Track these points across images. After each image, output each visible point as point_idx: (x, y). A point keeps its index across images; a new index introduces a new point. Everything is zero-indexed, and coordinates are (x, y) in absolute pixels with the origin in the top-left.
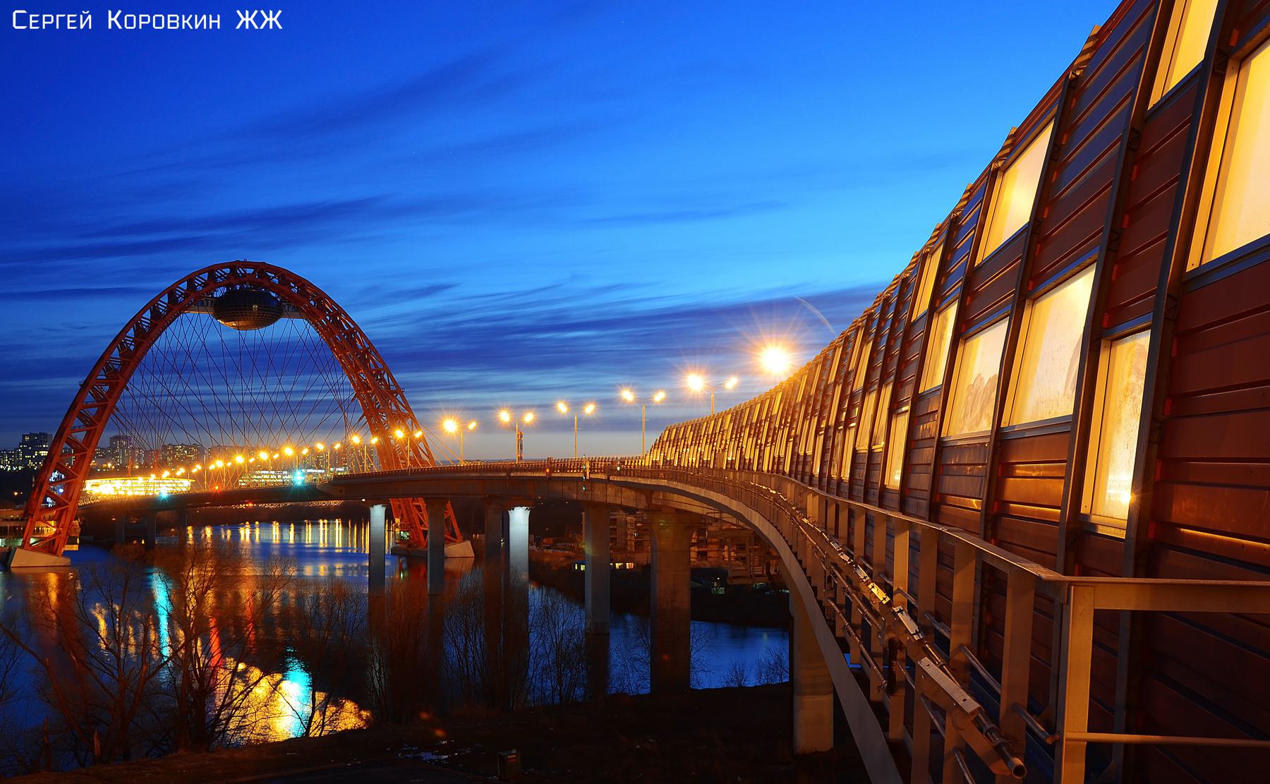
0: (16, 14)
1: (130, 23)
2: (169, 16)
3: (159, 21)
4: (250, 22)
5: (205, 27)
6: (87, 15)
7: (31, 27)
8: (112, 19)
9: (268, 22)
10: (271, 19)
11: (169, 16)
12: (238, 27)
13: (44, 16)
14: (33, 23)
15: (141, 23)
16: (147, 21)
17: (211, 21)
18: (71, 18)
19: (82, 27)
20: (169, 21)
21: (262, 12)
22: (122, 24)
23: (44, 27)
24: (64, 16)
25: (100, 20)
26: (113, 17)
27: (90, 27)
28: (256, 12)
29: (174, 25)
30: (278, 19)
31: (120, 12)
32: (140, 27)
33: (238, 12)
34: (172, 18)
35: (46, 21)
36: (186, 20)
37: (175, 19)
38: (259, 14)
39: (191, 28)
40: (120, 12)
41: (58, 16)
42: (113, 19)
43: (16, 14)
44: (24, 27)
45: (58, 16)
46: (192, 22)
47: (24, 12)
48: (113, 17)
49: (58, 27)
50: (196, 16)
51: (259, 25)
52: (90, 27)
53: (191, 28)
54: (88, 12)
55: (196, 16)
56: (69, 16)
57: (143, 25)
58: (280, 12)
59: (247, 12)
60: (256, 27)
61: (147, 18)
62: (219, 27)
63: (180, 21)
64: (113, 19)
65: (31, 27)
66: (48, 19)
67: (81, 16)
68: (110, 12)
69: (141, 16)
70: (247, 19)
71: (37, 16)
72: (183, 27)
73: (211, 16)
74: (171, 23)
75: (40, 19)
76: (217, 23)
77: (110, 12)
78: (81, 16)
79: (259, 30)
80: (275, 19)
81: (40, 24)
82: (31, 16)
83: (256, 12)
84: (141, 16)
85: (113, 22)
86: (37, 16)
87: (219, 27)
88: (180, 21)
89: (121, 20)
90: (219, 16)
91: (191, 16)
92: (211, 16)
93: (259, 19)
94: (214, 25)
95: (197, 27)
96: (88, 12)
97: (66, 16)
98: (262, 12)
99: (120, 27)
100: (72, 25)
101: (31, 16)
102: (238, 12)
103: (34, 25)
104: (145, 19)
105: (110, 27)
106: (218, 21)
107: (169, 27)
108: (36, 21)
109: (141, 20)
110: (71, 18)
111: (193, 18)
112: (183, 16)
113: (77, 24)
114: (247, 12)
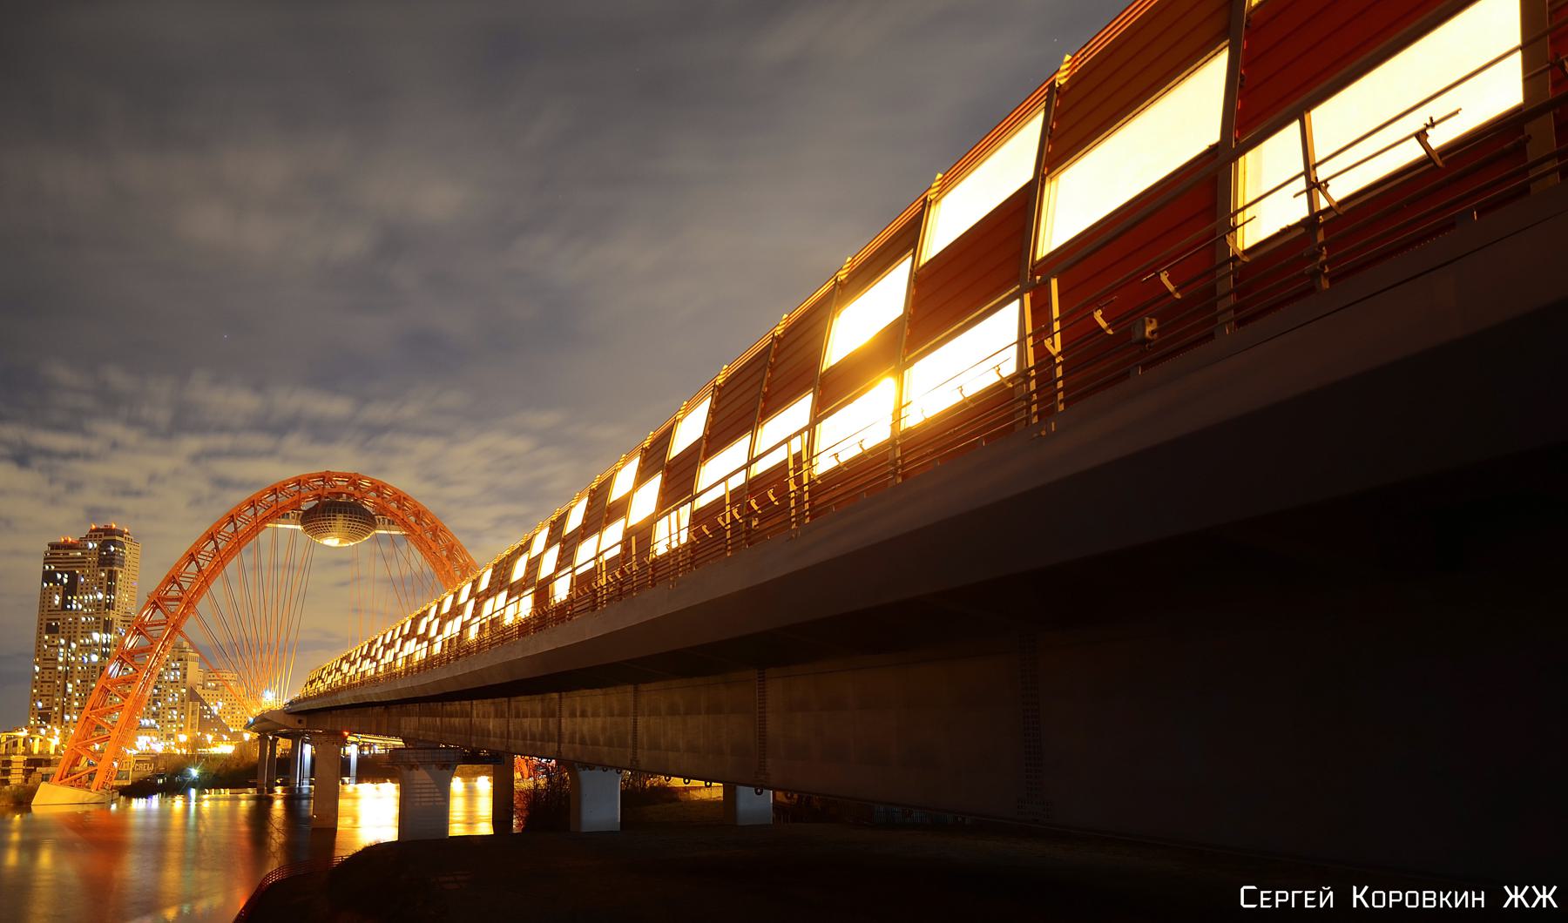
1: (1379, 901)
2: (1424, 893)
3: (1412, 899)
5: (1467, 906)
6: (1328, 891)
7: (1262, 906)
8: (1357, 896)
10: (1545, 896)
11: (1424, 893)
12: (1505, 906)
13: (1277, 893)
15: (1391, 900)
16: (1398, 898)
17: (1474, 899)
18: (1309, 896)
19: (1322, 905)
20: (1425, 899)
21: (1534, 888)
22: (1369, 902)
23: (1277, 906)
24: (1300, 892)
25: (1343, 897)
26: (1358, 893)
27: (1332, 906)
28: (1527, 888)
29: (1431, 903)
31: (1366, 888)
32: (1391, 906)
33: (1506, 888)
34: (1427, 896)
35: (1280, 898)
36: (1444, 897)
37: (1431, 896)
39: (1450, 906)
40: (1366, 888)
41: (1293, 893)
42: (1358, 896)
45: (1293, 893)
46: (1452, 899)
47: (1254, 888)
48: (1358, 893)
49: (1293, 906)
50: (1456, 893)
51: (1530, 904)
52: (1332, 906)
53: (1450, 906)
54: (1329, 888)
55: (1456, 893)
56: (1306, 893)
57: (1280, 903)
60: (1527, 906)
61: (1398, 894)
62: (1483, 906)
63: (1438, 899)
64: (1358, 896)
65: (1262, 906)
66: (1282, 896)
67: (1321, 893)
68: (1355, 888)
69: (1391, 893)
70: (1516, 896)
72: (1441, 906)
73: (1473, 893)
74: (1427, 901)
75: (1273, 896)
76: (1480, 901)
77: (1355, 888)
78: (1321, 893)
79: (1530, 909)
80: (1549, 896)
81: (1272, 902)
82: (1262, 893)
83: (1527, 888)
84: (1391, 893)
85: (1358, 900)
87: (1483, 906)
88: (1438, 899)
89: (1367, 897)
90: (1483, 893)
91: (1450, 893)
92: (1473, 893)
93: (1530, 897)
94: (1478, 903)
95: (1457, 905)
96: (1329, 888)
97: (1303, 893)
98: (1534, 888)
99: (1367, 906)
100: (1310, 903)
101: (1262, 893)
102: (1506, 888)
103: (1265, 903)
104: (1396, 896)
105: (1355, 906)
106: (1482, 899)
107: (1424, 906)
108: (1313, 899)
109: (1391, 898)
110: (1309, 896)
111: (1453, 895)
112: (1441, 893)
113: (1317, 902)
114: (1544, 888)
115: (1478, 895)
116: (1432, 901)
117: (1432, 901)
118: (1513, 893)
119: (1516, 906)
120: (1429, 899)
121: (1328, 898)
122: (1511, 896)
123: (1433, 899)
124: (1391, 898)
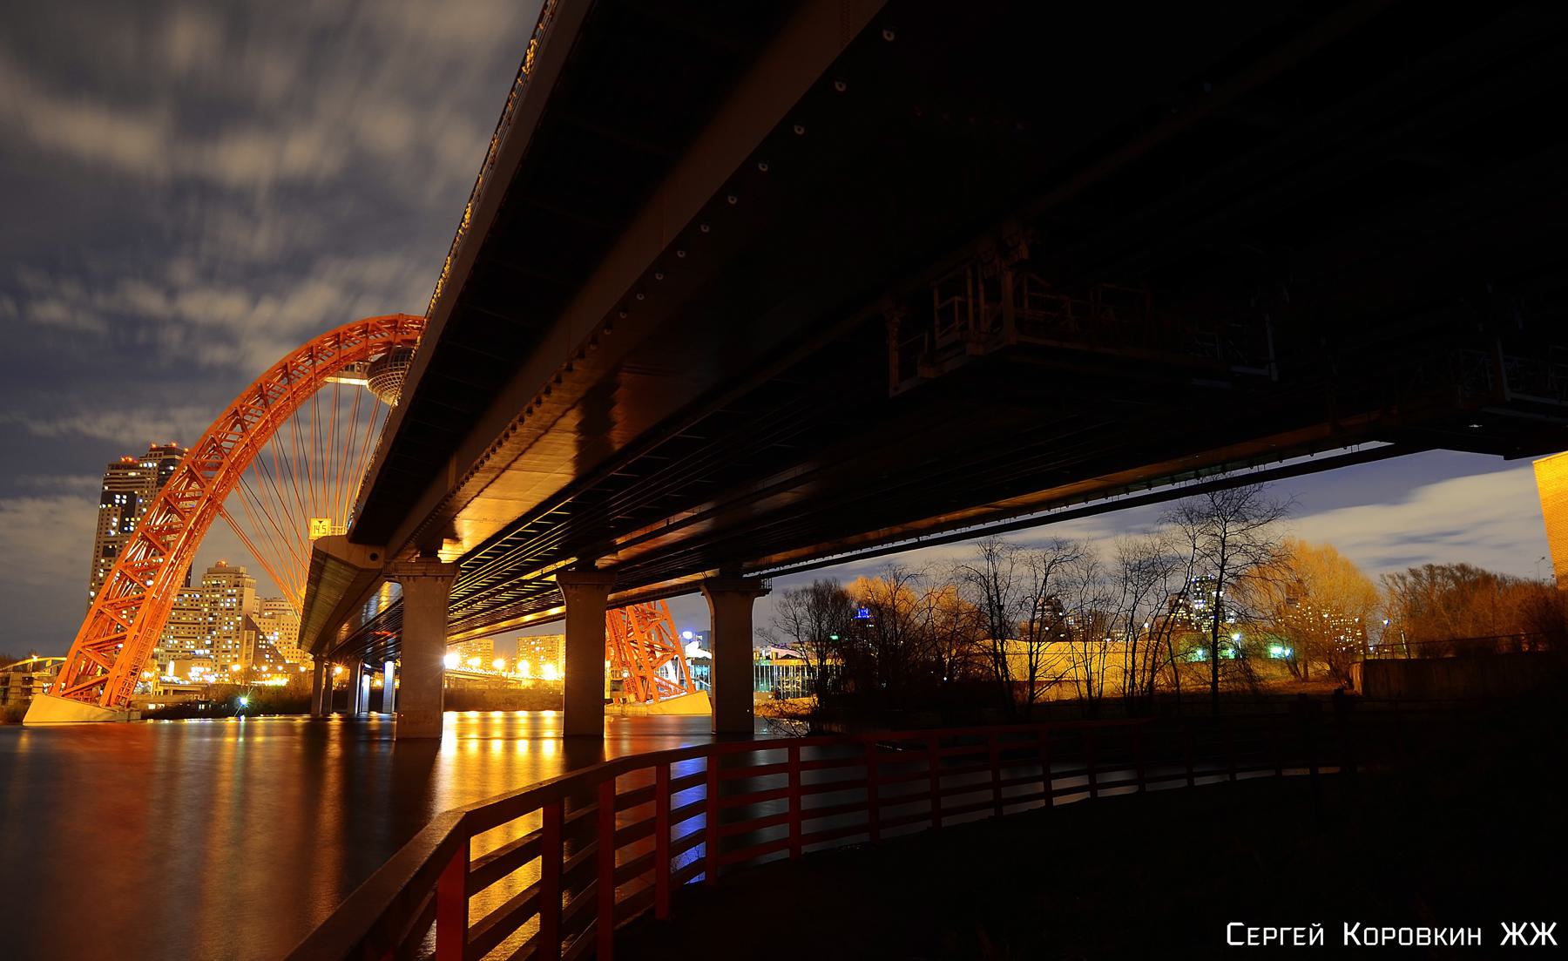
0: (1232, 927)
1: (1371, 938)
2: (1419, 929)
5: (1462, 944)
7: (1250, 943)
8: (1349, 933)
10: (1544, 933)
11: (1419, 929)
12: (1503, 943)
13: (1265, 929)
14: (1252, 938)
15: (1384, 938)
16: (1391, 935)
17: (1470, 936)
18: (1299, 933)
19: (1312, 942)
20: (1419, 936)
21: (1533, 924)
22: (1361, 939)
23: (1265, 944)
25: (1334, 934)
26: (1350, 930)
27: (1322, 943)
28: (1525, 924)
30: (1535, 933)
31: (1358, 924)
32: (1383, 944)
34: (1422, 933)
36: (1439, 934)
37: (1426, 933)
38: (1529, 927)
39: (1445, 944)
40: (1358, 924)
41: (1282, 929)
42: (1349, 934)
43: (1232, 927)
44: (1241, 943)
45: (1282, 929)
46: (1447, 936)
47: (1241, 924)
48: (1350, 930)
49: (1282, 943)
50: (1452, 930)
51: (1529, 940)
52: (1322, 943)
53: (1445, 944)
54: (1319, 924)
55: (1452, 930)
56: (1296, 929)
58: (1554, 924)
60: (1525, 943)
62: (1479, 943)
64: (1349, 934)
65: (1250, 943)
67: (1311, 930)
68: (1346, 925)
69: (1384, 929)
70: (1514, 933)
71: (1257, 929)
72: (1436, 943)
73: (1469, 930)
74: (1421, 938)
75: (1260, 933)
76: (1477, 938)
77: (1346, 925)
78: (1311, 930)
79: (1529, 946)
80: (1549, 934)
81: (1260, 939)
82: (1250, 929)
83: (1525, 924)
84: (1384, 929)
85: (1350, 937)
86: (1257, 929)
87: (1479, 943)
89: (1359, 934)
90: (1479, 930)
91: (1445, 929)
92: (1469, 930)
93: (1529, 934)
94: (1474, 940)
95: (1452, 942)
96: (1319, 924)
97: (1292, 931)
98: (1533, 924)
99: (1358, 943)
100: (1299, 940)
101: (1250, 929)
102: (1503, 924)
105: (1346, 943)
106: (1479, 936)
107: (1419, 943)
108: (1256, 936)
109: (1385, 935)
110: (1299, 933)
111: (1448, 932)
112: (1436, 930)
113: (1306, 939)
115: (1475, 932)
119: (1514, 943)
120: (1423, 936)
121: (1318, 936)
123: (1428, 936)
124: (1385, 935)
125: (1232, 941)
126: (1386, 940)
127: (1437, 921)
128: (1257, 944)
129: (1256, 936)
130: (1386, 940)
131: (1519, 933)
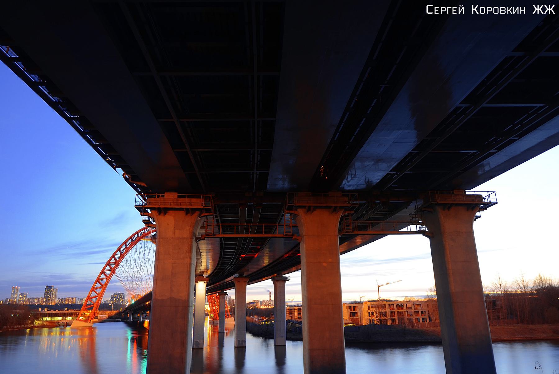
2: (501, 8)
4: (539, 10)
5: (518, 13)
6: (462, 7)
7: (435, 13)
8: (474, 9)
9: (548, 10)
10: (550, 9)
11: (501, 8)
12: (534, 13)
13: (441, 8)
15: (487, 11)
16: (490, 10)
17: (521, 10)
18: (454, 9)
19: (459, 13)
20: (501, 10)
21: (545, 6)
22: (479, 11)
23: (441, 13)
24: (451, 7)
25: (468, 10)
26: (474, 8)
27: (463, 13)
28: (542, 6)
29: (503, 12)
31: (477, 6)
32: (487, 13)
33: (534, 6)
34: (502, 9)
35: (442, 10)
36: (509, 9)
37: (504, 9)
38: (544, 7)
39: (511, 13)
40: (477, 6)
41: (448, 8)
42: (474, 9)
44: (432, 13)
45: (448, 8)
46: (512, 10)
47: (432, 6)
48: (474, 8)
49: (448, 13)
50: (514, 8)
51: (544, 12)
52: (463, 13)
53: (511, 13)
54: (462, 6)
55: (514, 8)
56: (453, 8)
58: (554, 6)
59: (538, 6)
60: (542, 13)
61: (490, 8)
62: (525, 13)
63: (506, 10)
64: (474, 9)
65: (435, 13)
66: (443, 9)
67: (459, 8)
68: (473, 6)
69: (487, 8)
70: (538, 9)
71: (438, 7)
72: (508, 13)
73: (521, 8)
75: (439, 9)
76: (524, 11)
77: (473, 6)
78: (459, 8)
80: (551, 9)
81: (439, 11)
82: (435, 8)
83: (542, 6)
84: (487, 8)
85: (474, 11)
86: (438, 7)
87: (525, 13)
88: (506, 10)
89: (478, 9)
90: (525, 8)
91: (511, 8)
92: (521, 8)
94: (523, 12)
95: (514, 13)
96: (462, 6)
97: (452, 8)
98: (545, 6)
99: (478, 13)
100: (454, 12)
101: (435, 8)
102: (534, 6)
103: (437, 12)
104: (489, 9)
105: (473, 13)
106: (524, 10)
107: (501, 13)
108: (438, 10)
109: (488, 10)
110: (454, 9)
111: (512, 9)
112: (508, 8)
113: (457, 11)
115: (523, 9)
116: (504, 11)
117: (504, 11)
118: (548, 8)
120: (503, 10)
122: (536, 9)
123: (505, 10)
124: (488, 10)
125: (428, 12)
126: (488, 12)
127: (507, 5)
128: (438, 13)
129: (438, 10)
130: (488, 12)
131: (540, 9)
